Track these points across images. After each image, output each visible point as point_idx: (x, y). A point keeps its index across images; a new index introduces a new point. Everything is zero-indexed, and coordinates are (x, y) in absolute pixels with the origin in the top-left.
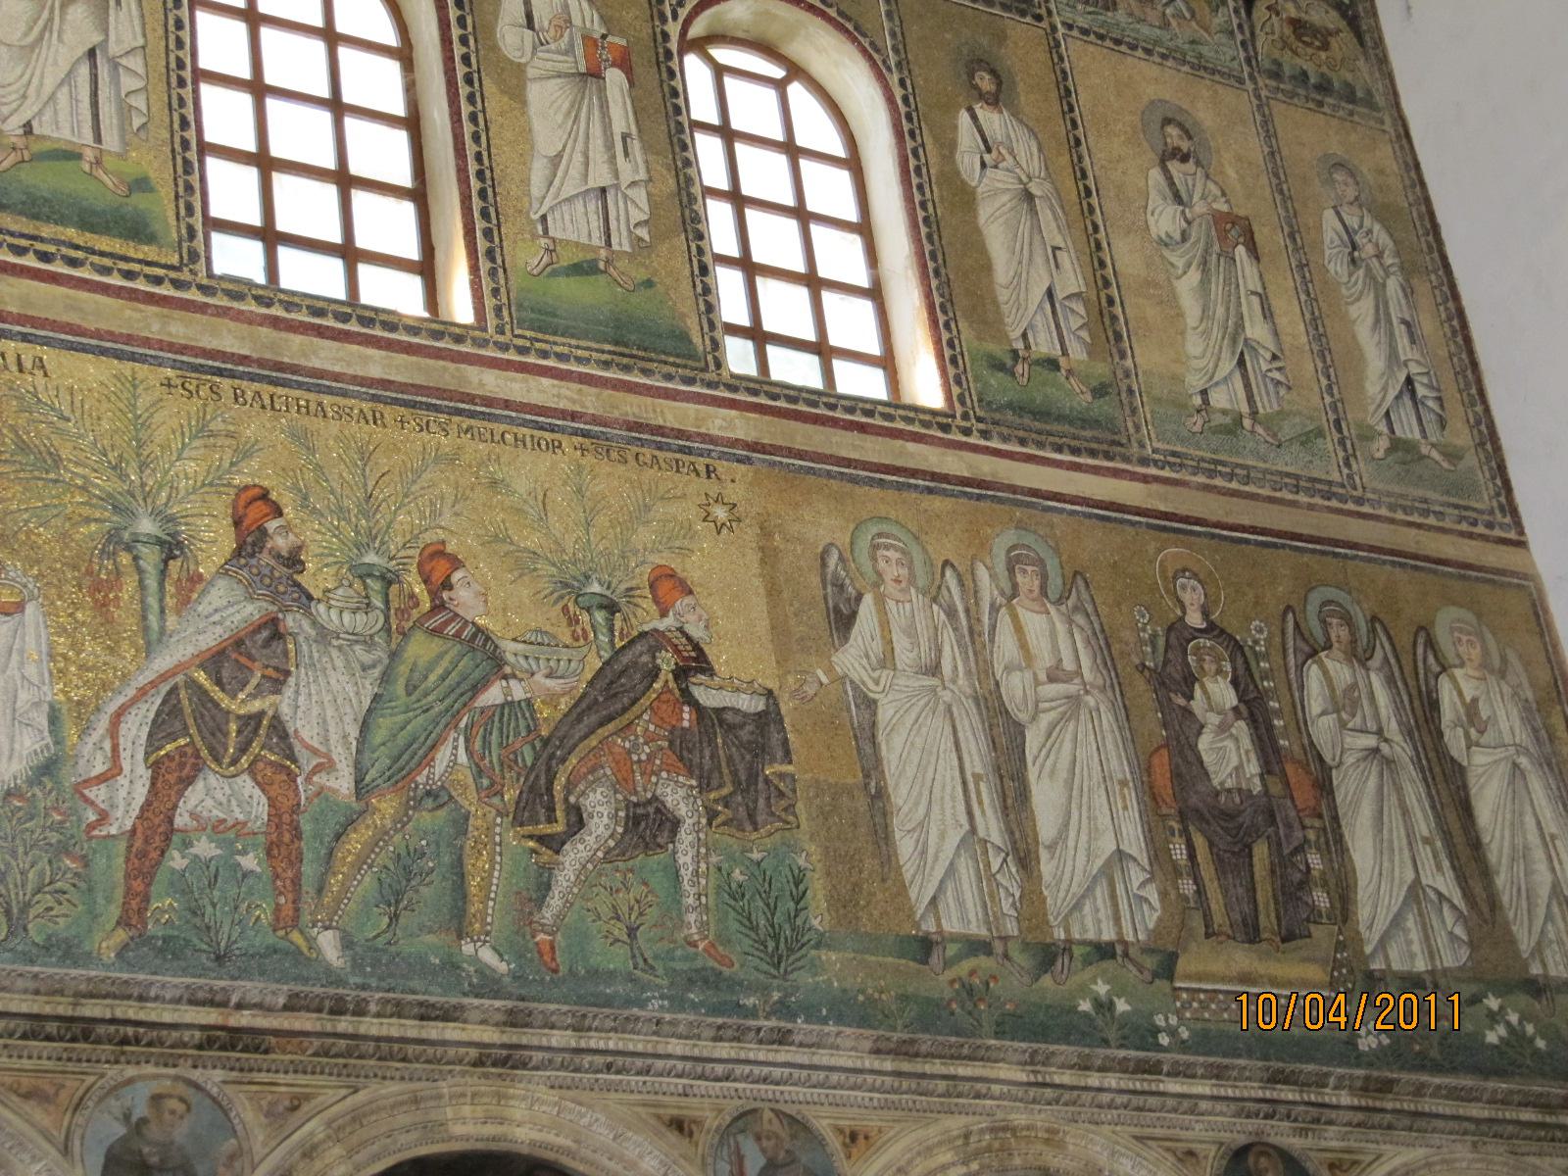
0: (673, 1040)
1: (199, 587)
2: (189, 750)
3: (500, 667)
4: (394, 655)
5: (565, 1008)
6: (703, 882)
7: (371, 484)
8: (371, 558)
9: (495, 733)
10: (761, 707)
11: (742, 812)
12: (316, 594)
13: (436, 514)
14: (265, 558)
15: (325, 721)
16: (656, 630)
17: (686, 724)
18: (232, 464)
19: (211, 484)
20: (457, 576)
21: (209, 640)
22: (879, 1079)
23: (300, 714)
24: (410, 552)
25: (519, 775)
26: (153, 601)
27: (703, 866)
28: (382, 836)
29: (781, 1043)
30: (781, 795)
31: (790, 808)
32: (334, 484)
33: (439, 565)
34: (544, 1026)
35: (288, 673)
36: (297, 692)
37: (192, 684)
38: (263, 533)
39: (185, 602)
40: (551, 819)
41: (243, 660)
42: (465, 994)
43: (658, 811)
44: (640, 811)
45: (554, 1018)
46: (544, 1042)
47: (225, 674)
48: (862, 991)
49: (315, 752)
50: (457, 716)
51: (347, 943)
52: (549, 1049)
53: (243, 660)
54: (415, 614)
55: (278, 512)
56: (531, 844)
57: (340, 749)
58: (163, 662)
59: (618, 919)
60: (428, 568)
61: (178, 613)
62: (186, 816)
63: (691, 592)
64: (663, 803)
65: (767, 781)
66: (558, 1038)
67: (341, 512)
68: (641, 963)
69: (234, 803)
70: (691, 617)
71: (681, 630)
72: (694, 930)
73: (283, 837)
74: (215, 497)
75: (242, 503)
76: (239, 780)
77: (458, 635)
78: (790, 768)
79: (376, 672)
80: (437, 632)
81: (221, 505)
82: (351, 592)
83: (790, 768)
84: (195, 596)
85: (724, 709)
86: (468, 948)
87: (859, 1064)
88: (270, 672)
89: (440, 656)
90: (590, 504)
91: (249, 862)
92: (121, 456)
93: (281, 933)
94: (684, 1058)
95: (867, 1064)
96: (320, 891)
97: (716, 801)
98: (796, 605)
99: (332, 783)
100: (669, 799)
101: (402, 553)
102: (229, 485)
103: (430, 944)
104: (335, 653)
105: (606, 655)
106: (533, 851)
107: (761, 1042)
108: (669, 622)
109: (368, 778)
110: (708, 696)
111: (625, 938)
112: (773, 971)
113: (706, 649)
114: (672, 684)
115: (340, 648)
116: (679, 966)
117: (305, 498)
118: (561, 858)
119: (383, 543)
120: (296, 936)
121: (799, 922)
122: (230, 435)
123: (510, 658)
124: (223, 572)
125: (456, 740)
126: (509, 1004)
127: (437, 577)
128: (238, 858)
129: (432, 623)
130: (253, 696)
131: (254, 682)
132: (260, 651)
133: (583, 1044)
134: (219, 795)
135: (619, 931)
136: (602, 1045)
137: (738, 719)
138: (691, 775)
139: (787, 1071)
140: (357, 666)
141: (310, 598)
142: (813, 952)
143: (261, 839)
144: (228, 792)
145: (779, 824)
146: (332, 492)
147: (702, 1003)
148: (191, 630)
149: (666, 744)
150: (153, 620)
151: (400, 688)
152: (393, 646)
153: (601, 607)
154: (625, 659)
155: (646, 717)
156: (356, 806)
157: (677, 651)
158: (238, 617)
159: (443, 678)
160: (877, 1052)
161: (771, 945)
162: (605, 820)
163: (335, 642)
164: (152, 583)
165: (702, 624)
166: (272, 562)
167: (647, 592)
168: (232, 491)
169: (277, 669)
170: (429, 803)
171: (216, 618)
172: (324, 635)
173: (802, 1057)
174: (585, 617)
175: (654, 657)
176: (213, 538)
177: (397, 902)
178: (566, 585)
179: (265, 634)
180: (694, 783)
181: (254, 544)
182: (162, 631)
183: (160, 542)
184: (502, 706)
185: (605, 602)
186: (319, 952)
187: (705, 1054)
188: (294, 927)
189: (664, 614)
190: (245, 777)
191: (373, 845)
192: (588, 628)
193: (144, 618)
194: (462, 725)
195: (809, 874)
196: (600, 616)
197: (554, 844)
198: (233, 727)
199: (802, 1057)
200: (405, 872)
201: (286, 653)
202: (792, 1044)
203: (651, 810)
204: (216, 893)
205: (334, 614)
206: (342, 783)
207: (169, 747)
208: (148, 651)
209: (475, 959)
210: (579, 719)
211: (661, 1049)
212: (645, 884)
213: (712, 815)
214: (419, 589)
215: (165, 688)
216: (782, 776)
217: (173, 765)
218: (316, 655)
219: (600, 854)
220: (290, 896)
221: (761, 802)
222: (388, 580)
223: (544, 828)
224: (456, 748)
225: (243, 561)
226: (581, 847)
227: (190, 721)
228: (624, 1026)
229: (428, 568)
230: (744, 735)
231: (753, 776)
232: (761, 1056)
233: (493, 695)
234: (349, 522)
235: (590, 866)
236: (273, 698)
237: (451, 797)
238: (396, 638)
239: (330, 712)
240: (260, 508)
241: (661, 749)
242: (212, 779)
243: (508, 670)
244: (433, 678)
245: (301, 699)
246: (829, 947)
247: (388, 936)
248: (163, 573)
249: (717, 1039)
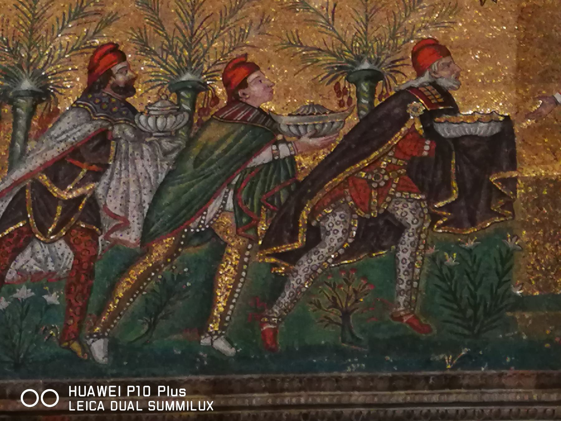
0: (356, 393)
1: (55, 119)
2: (25, 230)
3: (274, 136)
4: (190, 142)
5: (255, 376)
6: (417, 271)
7: (196, 25)
8: (187, 77)
9: (260, 184)
10: (497, 130)
11: (464, 214)
12: (139, 108)
13: (244, 36)
14: (108, 91)
15: (127, 196)
16: (411, 88)
17: (425, 153)
18: (95, 33)
19: (78, 49)
20: (254, 76)
21: (53, 153)
22: (549, 409)
23: (110, 192)
24: (218, 67)
25: (272, 211)
26: (20, 134)
27: (419, 258)
28: (156, 267)
29: (451, 388)
30: (502, 195)
31: (509, 205)
32: (168, 31)
33: (238, 72)
34: (245, 392)
35: (108, 166)
36: (111, 178)
37: (37, 186)
38: (109, 74)
39: (43, 130)
40: (293, 239)
41: (76, 163)
42: (196, 373)
43: (387, 222)
44: (371, 224)
45: (251, 384)
46: (247, 402)
47: (61, 174)
48: (550, 340)
49: (115, 217)
50: (233, 176)
51: (113, 347)
52: (251, 407)
53: (76, 163)
54: (215, 110)
55: (122, 57)
56: (273, 260)
57: (135, 213)
58: (18, 173)
59: (335, 305)
60: (229, 75)
61: (37, 139)
62: (14, 274)
63: (448, 54)
64: (393, 216)
65: (491, 186)
66: (257, 399)
67: (171, 50)
68: (349, 338)
69: (50, 259)
70: (445, 73)
71: (434, 84)
72: (402, 308)
73: (80, 280)
74: (78, 58)
75: (97, 57)
76: (56, 244)
77: (244, 119)
78: (515, 174)
79: (174, 155)
80: (230, 119)
81: (81, 62)
82: (167, 103)
83: (515, 174)
84: (50, 126)
85: (463, 137)
86: (205, 341)
87: (526, 398)
88: (94, 167)
89: (227, 136)
90: (372, 6)
91: (52, 298)
92: (17, 43)
93: (66, 344)
94: (365, 405)
95: (535, 397)
96: (100, 314)
97: (440, 208)
98: (546, 46)
99: (125, 237)
100: (399, 212)
101: (213, 69)
102: (91, 47)
103: (175, 342)
104: (145, 147)
105: (363, 113)
106: (274, 265)
107: (431, 388)
108: (426, 78)
109: (152, 230)
110: (446, 129)
111: (340, 320)
112: (466, 332)
113: (456, 96)
114: (419, 126)
115: (150, 143)
116: (380, 336)
117: (146, 45)
118: (296, 267)
119: (198, 65)
120: (75, 346)
121: (500, 291)
122: (97, 13)
123: (284, 129)
124: (76, 106)
125: (227, 193)
126: (212, 377)
127: (236, 81)
128: (45, 297)
129: (227, 114)
130: (77, 186)
131: (81, 175)
132: (93, 155)
133: (278, 402)
134: (40, 256)
135: (335, 314)
136: (294, 401)
137: (473, 143)
138: (421, 191)
139: (461, 408)
140: (160, 154)
141: (134, 111)
142: (509, 314)
143: (64, 282)
144: (47, 252)
145: (497, 220)
146: (167, 38)
147: (395, 363)
148: (43, 148)
149: (402, 171)
150: (18, 146)
151: (189, 164)
152: (192, 135)
153: (367, 79)
154: (380, 114)
155: (390, 154)
156: (138, 251)
157: (428, 101)
158: (79, 134)
159: (225, 151)
160: (540, 386)
161: (470, 312)
162: (340, 235)
163: (148, 140)
164: (22, 122)
165: (453, 76)
166: (111, 93)
167: (409, 61)
168: (91, 50)
169: (98, 164)
170: (196, 241)
171: (64, 136)
172: (140, 135)
173: (473, 397)
174: (353, 89)
175: (406, 108)
176: (74, 84)
177: (157, 313)
178: (340, 68)
179: (96, 143)
180: (423, 197)
181: (101, 83)
182: (24, 151)
183: (32, 93)
184: (269, 164)
185: (369, 73)
186: (90, 354)
187: (384, 400)
188: (74, 340)
189: (420, 74)
190: (62, 242)
191: (142, 278)
192: (354, 96)
193: (12, 145)
194: (234, 182)
195: (516, 253)
196: (365, 87)
197: (293, 258)
198: (59, 208)
199: (473, 397)
200: (169, 290)
201: (108, 155)
202: (460, 387)
203: (381, 223)
204: (25, 322)
205: (151, 121)
206: (132, 236)
207: (12, 228)
208: (11, 169)
209: (210, 347)
210: (333, 163)
211: (345, 400)
212: (365, 277)
213: (435, 217)
214: (220, 91)
215: (16, 190)
216: (504, 181)
217: (11, 240)
218: (131, 151)
219: (330, 261)
220: (77, 319)
221: (482, 202)
222: (197, 88)
223: (287, 248)
224: (225, 199)
225: (90, 96)
226: (314, 257)
227: (29, 209)
228: (311, 385)
229: (229, 75)
230: (477, 154)
231: (479, 183)
232: (435, 398)
233: (265, 156)
234: (174, 54)
235: (319, 271)
236: (91, 186)
237: (215, 235)
238: (195, 129)
239: (132, 189)
240: (111, 57)
241: (399, 175)
242: (37, 246)
243: (280, 137)
244: (217, 152)
245: (114, 183)
246: (524, 309)
247: (146, 338)
248: (31, 113)
249: (392, 388)
